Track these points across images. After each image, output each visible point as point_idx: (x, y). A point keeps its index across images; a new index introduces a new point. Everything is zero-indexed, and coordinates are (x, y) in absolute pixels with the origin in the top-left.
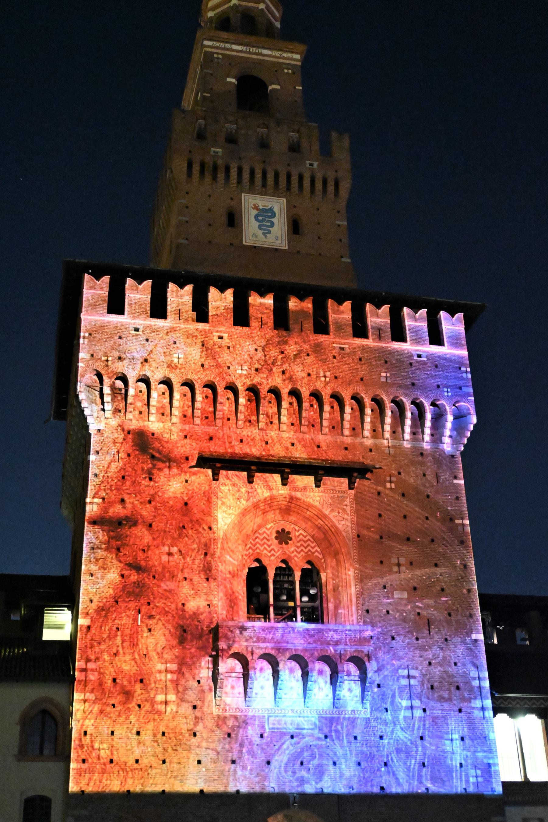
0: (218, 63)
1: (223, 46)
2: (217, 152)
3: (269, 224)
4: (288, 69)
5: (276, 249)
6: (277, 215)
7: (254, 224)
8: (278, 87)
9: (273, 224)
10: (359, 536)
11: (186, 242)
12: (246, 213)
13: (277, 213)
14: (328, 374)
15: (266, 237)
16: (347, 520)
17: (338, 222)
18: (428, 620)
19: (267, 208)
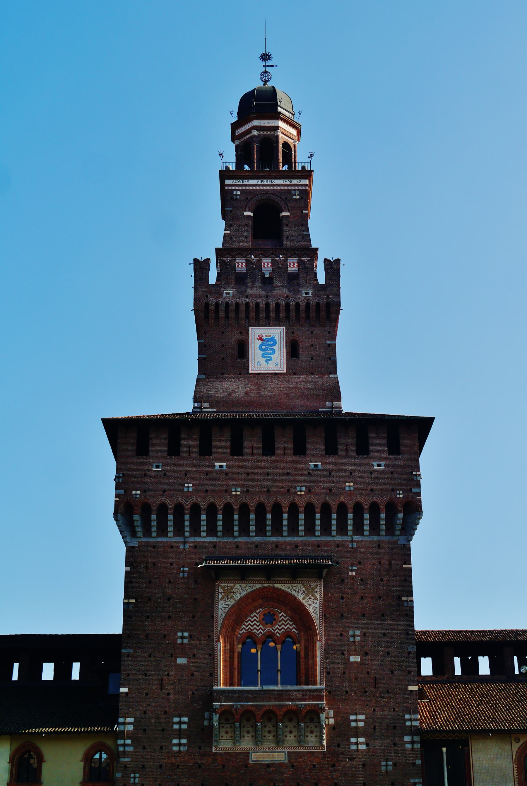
0: (237, 199)
1: (241, 183)
2: (229, 293)
3: (271, 352)
4: (295, 195)
5: (276, 374)
6: (277, 343)
7: (259, 353)
8: (288, 214)
9: (274, 351)
10: (325, 616)
11: (203, 377)
12: (253, 345)
13: (277, 341)
14: (304, 488)
15: (268, 363)
16: (316, 603)
17: (328, 342)
18: (375, 677)
19: (269, 337)
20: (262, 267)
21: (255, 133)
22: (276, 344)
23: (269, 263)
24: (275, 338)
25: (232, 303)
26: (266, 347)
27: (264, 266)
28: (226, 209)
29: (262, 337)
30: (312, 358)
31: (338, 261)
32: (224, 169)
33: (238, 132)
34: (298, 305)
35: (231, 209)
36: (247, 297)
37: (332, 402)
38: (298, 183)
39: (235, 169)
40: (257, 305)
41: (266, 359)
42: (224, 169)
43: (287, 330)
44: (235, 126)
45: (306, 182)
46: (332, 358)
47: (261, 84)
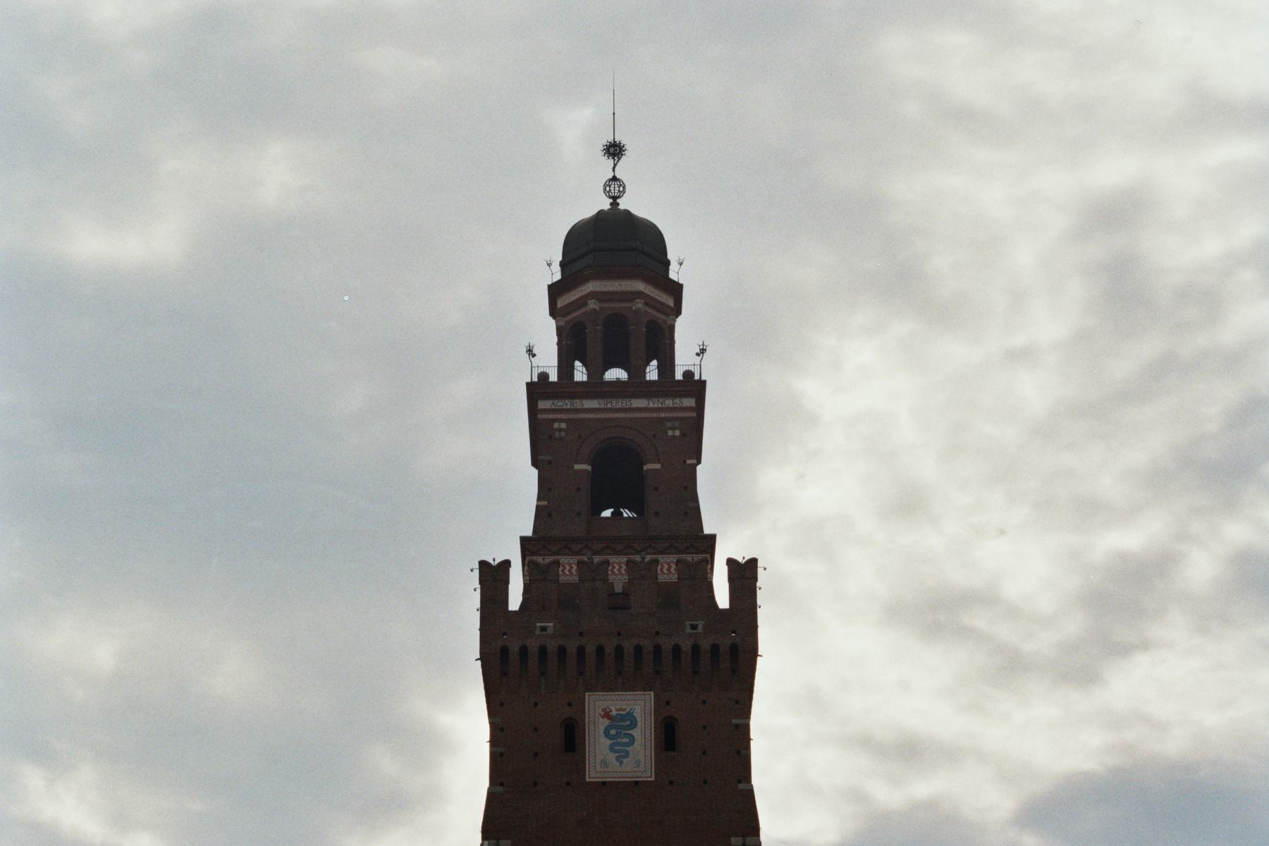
1: (568, 407)
3: (626, 740)
4: (673, 429)
5: (637, 783)
6: (639, 724)
8: (658, 466)
12: (592, 728)
13: (639, 720)
15: (621, 763)
17: (735, 721)
19: (624, 713)
20: (610, 572)
21: (593, 305)
22: (636, 725)
23: (622, 565)
24: (635, 714)
25: (552, 646)
26: (617, 732)
27: (612, 570)
28: (540, 458)
29: (609, 712)
30: (704, 753)
31: (753, 563)
32: (535, 379)
33: (560, 303)
34: (677, 649)
35: (548, 458)
36: (581, 634)
37: (744, 836)
38: (676, 405)
39: (556, 380)
40: (600, 650)
41: (617, 754)
42: (536, 380)
43: (657, 698)
44: (555, 291)
45: (690, 402)
46: (743, 752)
47: (605, 204)
